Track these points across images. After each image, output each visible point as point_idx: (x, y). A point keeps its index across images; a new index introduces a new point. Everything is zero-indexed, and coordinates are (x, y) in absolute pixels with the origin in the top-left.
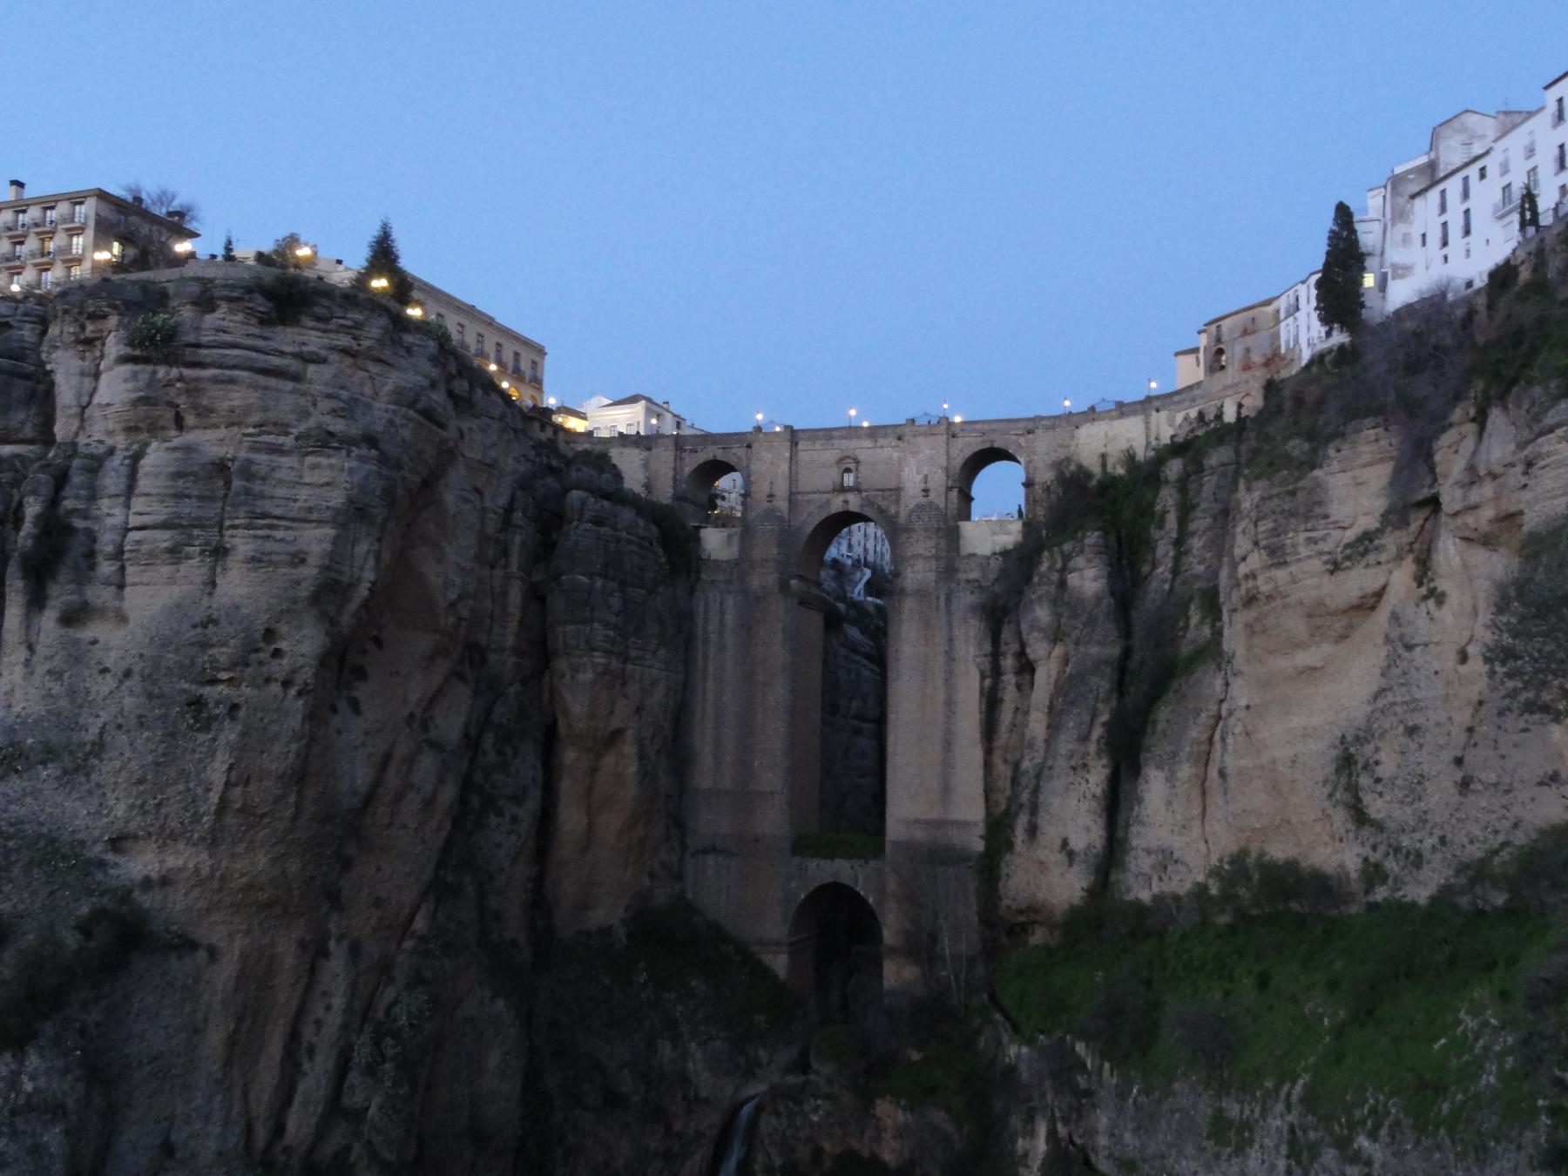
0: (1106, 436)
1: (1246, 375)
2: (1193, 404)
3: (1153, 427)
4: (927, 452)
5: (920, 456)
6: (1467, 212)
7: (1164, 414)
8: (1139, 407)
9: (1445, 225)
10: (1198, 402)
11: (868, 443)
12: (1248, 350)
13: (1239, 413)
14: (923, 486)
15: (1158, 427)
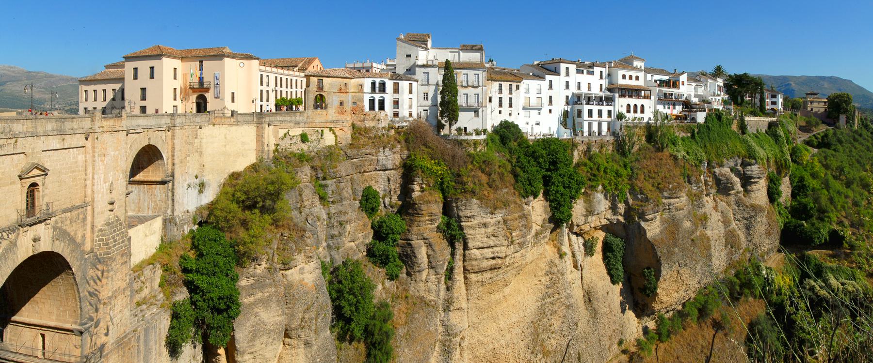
0: (226, 138)
1: (340, 117)
2: (297, 126)
3: (266, 136)
4: (112, 153)
5: (107, 159)
6: (511, 99)
7: (271, 127)
8: (250, 118)
9: (501, 99)
10: (302, 125)
11: (54, 142)
12: (342, 103)
13: (336, 140)
14: (108, 198)
15: (268, 136)
